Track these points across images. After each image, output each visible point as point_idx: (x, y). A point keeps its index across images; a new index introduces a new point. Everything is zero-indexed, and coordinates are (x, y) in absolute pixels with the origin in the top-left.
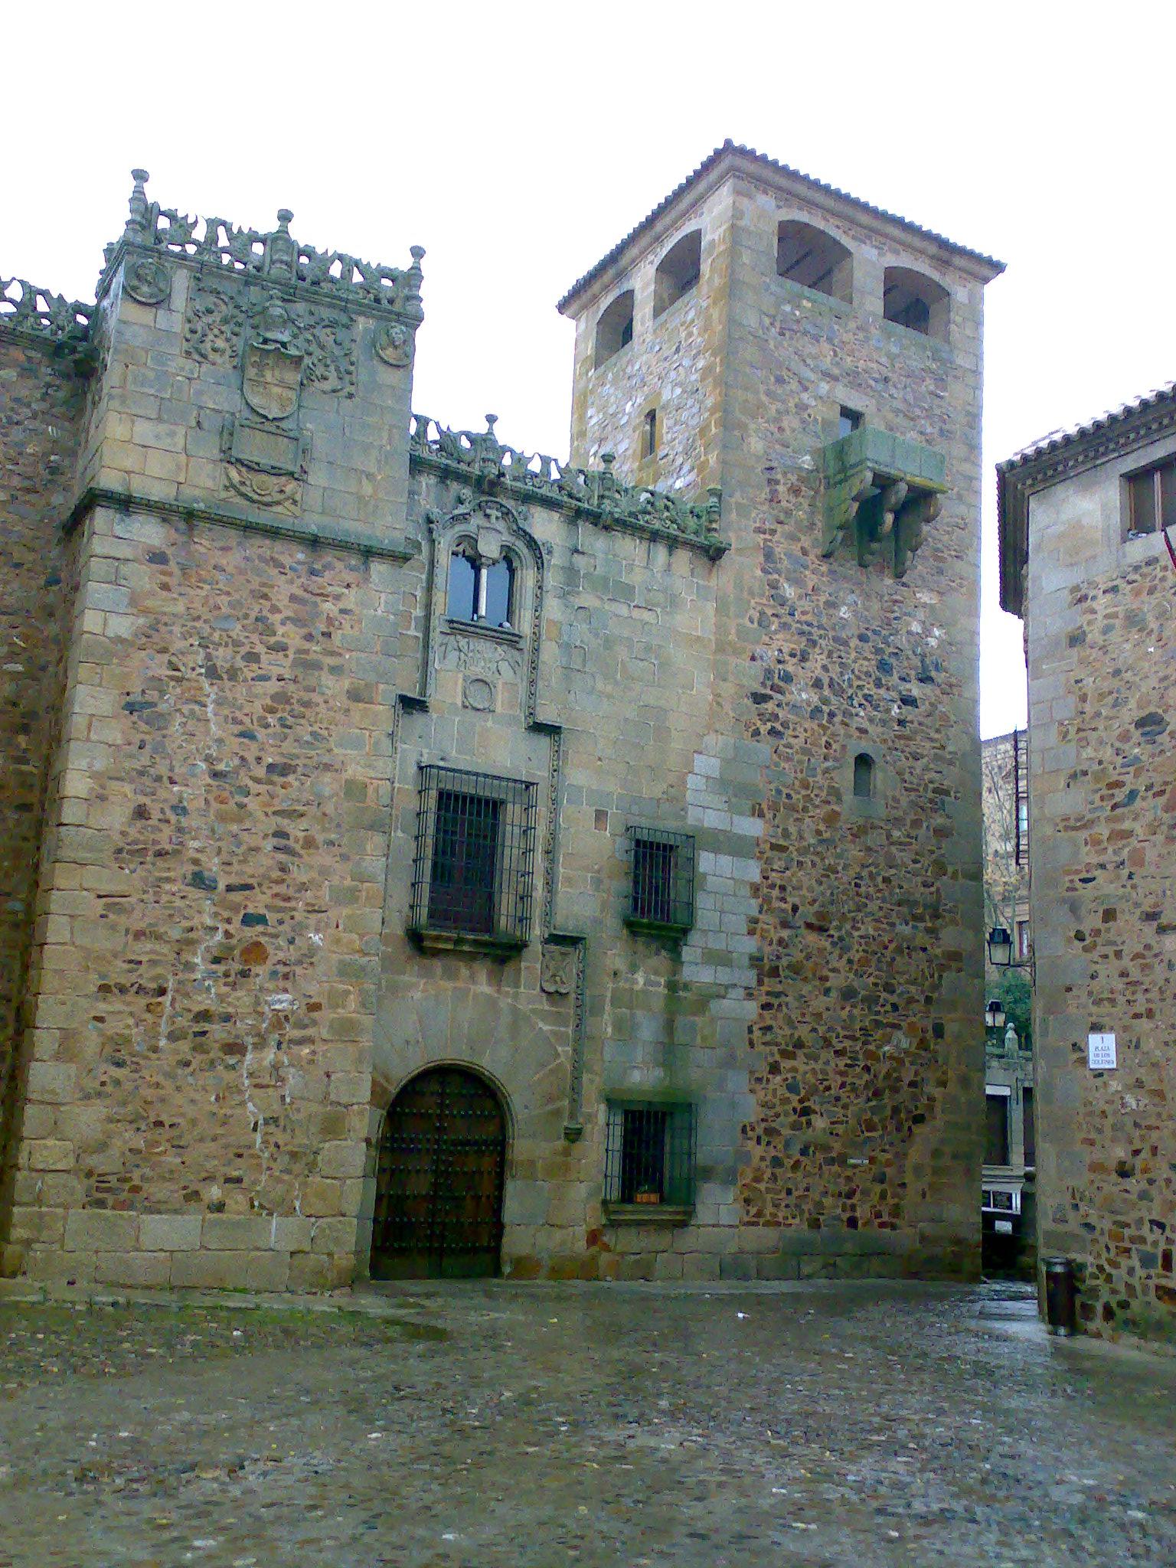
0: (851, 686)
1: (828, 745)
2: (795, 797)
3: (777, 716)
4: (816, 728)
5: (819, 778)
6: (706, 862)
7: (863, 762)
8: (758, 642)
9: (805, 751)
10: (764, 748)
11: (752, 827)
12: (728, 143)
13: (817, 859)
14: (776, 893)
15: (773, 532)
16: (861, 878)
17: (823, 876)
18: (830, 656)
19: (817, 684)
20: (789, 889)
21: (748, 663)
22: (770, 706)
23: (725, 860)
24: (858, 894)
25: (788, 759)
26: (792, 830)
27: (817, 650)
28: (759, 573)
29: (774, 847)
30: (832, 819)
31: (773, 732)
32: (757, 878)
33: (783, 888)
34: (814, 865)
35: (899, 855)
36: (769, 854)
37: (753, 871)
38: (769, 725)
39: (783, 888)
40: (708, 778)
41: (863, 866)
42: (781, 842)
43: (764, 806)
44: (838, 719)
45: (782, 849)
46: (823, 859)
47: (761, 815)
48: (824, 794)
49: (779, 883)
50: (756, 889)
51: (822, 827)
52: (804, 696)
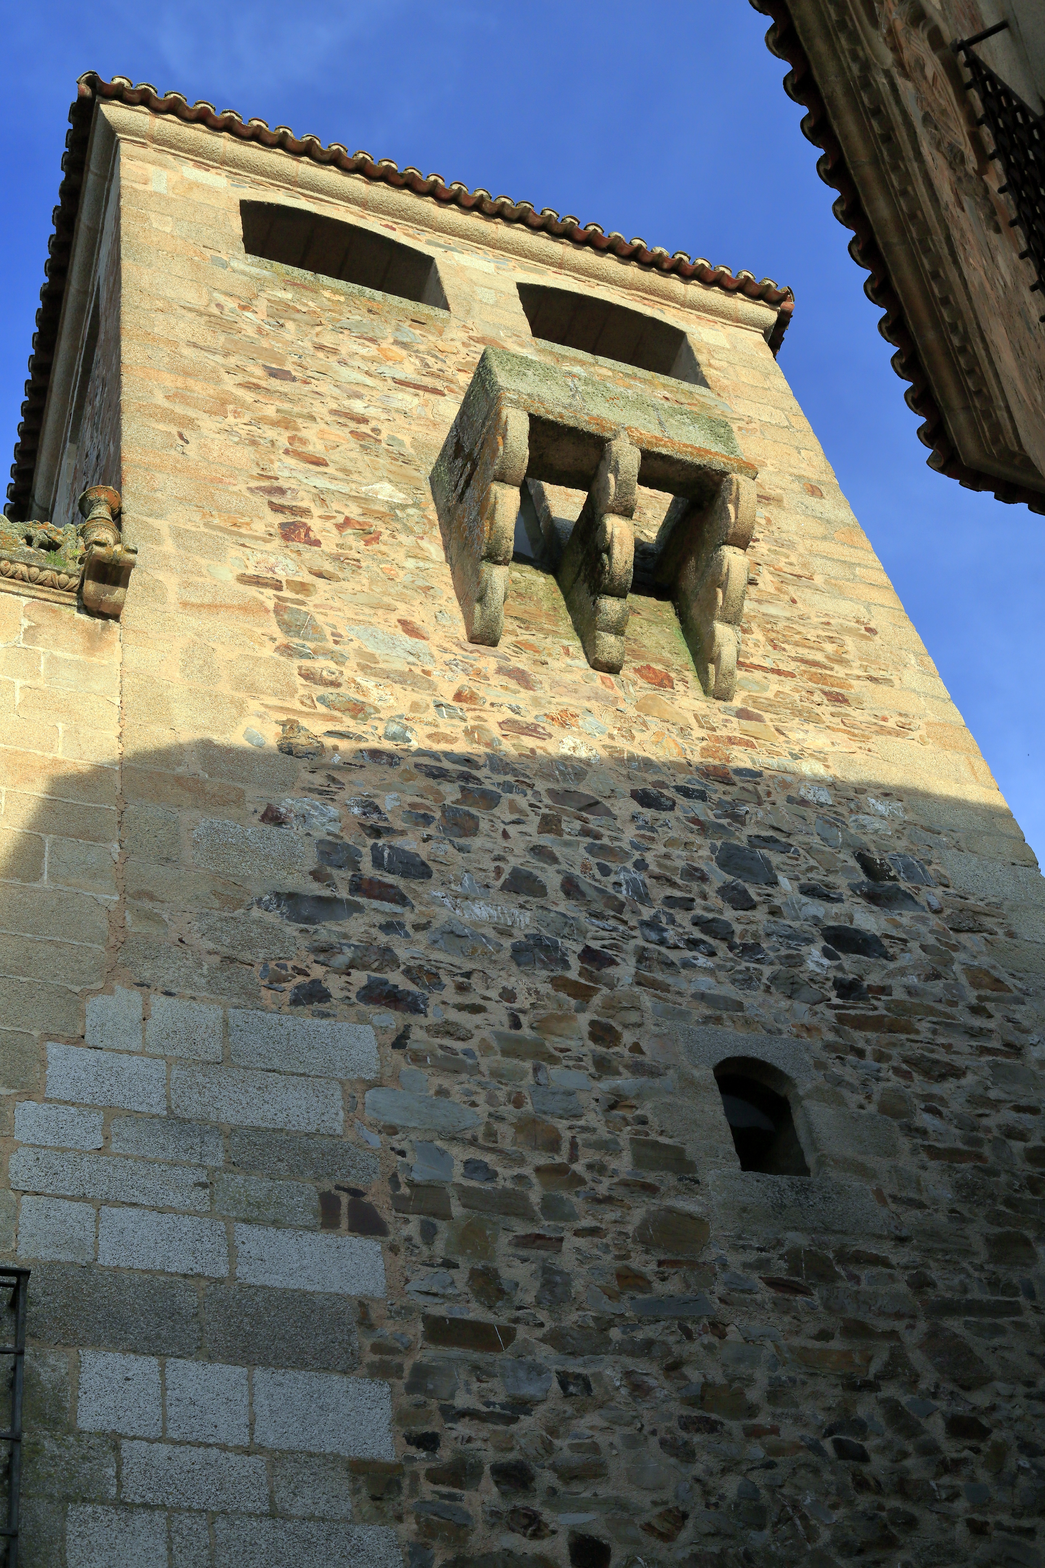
0: (644, 898)
1: (602, 1033)
2: (505, 1174)
3: (387, 957)
4: (546, 988)
5: (593, 1118)
6: (106, 1387)
7: (755, 1097)
8: (285, 785)
9: (512, 1048)
10: (358, 1038)
11: (345, 1267)
12: (93, 81)
13: (648, 1369)
14: (483, 1497)
15: (303, 588)
16: (860, 1427)
17: (686, 1424)
18: (549, 824)
19: (522, 884)
20: (546, 1478)
21: (254, 828)
22: (356, 927)
23: (209, 1389)
24: (861, 1484)
25: (452, 1065)
26: (519, 1273)
27: (503, 812)
28: (268, 651)
29: (440, 1331)
30: (675, 1237)
31: (381, 995)
32: (383, 1445)
33: (514, 1477)
34: (638, 1389)
35: (979, 1346)
36: (429, 1354)
37: (361, 1418)
38: (360, 978)
39: (514, 1477)
40: (111, 1112)
41: (857, 1386)
42: (476, 1312)
43: (378, 1197)
44: (625, 971)
45: (480, 1336)
46: (673, 1368)
47: (366, 1223)
48: (623, 1164)
49: (490, 1456)
50: (377, 1483)
51: (643, 1263)
52: (481, 911)
